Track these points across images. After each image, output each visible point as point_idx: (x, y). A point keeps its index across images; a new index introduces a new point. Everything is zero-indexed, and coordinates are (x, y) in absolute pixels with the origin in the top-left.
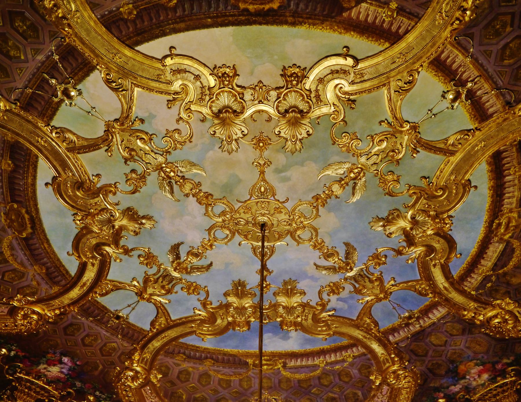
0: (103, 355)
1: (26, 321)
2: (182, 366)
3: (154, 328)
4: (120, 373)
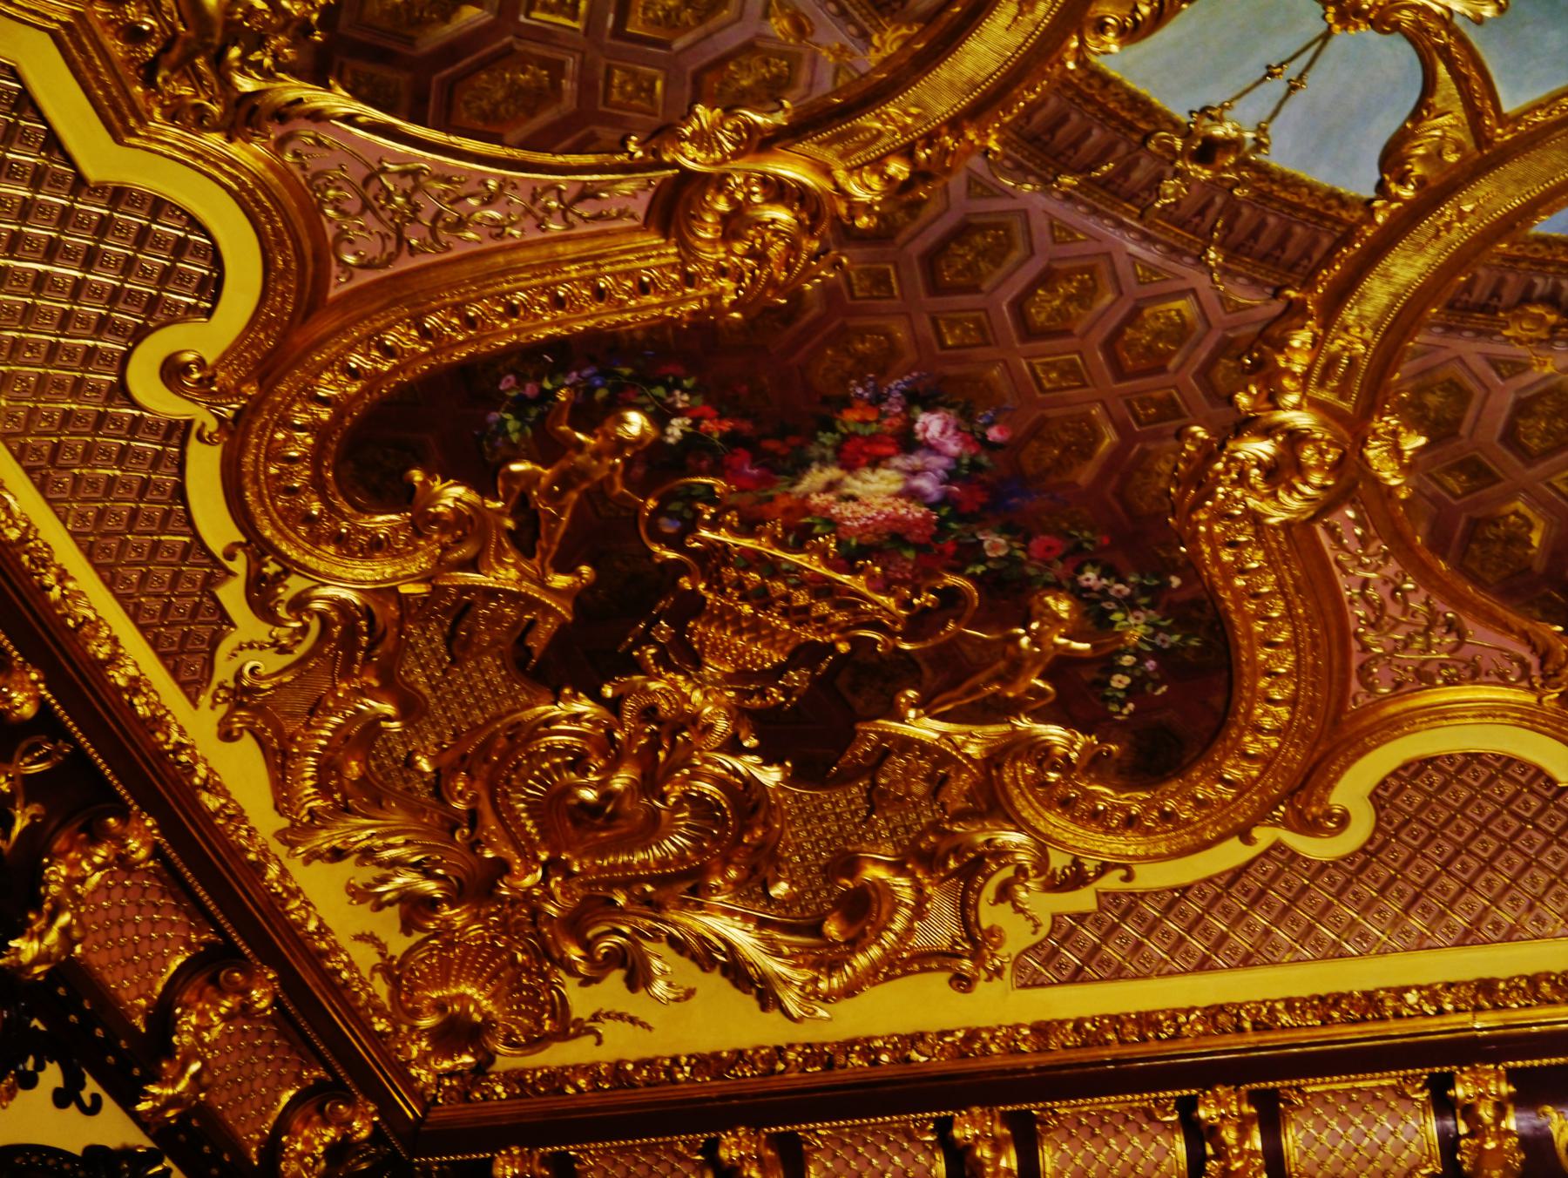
0: (1120, 373)
1: (739, 247)
2: (1537, 372)
3: (1402, 181)
4: (1209, 453)
